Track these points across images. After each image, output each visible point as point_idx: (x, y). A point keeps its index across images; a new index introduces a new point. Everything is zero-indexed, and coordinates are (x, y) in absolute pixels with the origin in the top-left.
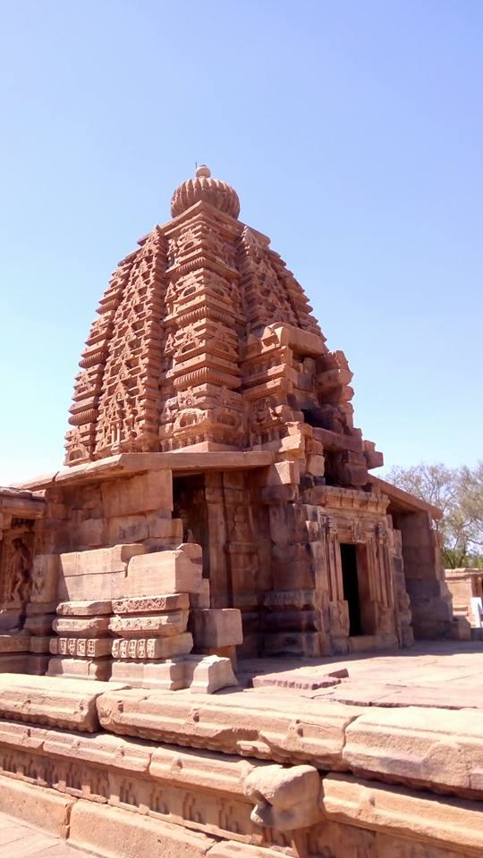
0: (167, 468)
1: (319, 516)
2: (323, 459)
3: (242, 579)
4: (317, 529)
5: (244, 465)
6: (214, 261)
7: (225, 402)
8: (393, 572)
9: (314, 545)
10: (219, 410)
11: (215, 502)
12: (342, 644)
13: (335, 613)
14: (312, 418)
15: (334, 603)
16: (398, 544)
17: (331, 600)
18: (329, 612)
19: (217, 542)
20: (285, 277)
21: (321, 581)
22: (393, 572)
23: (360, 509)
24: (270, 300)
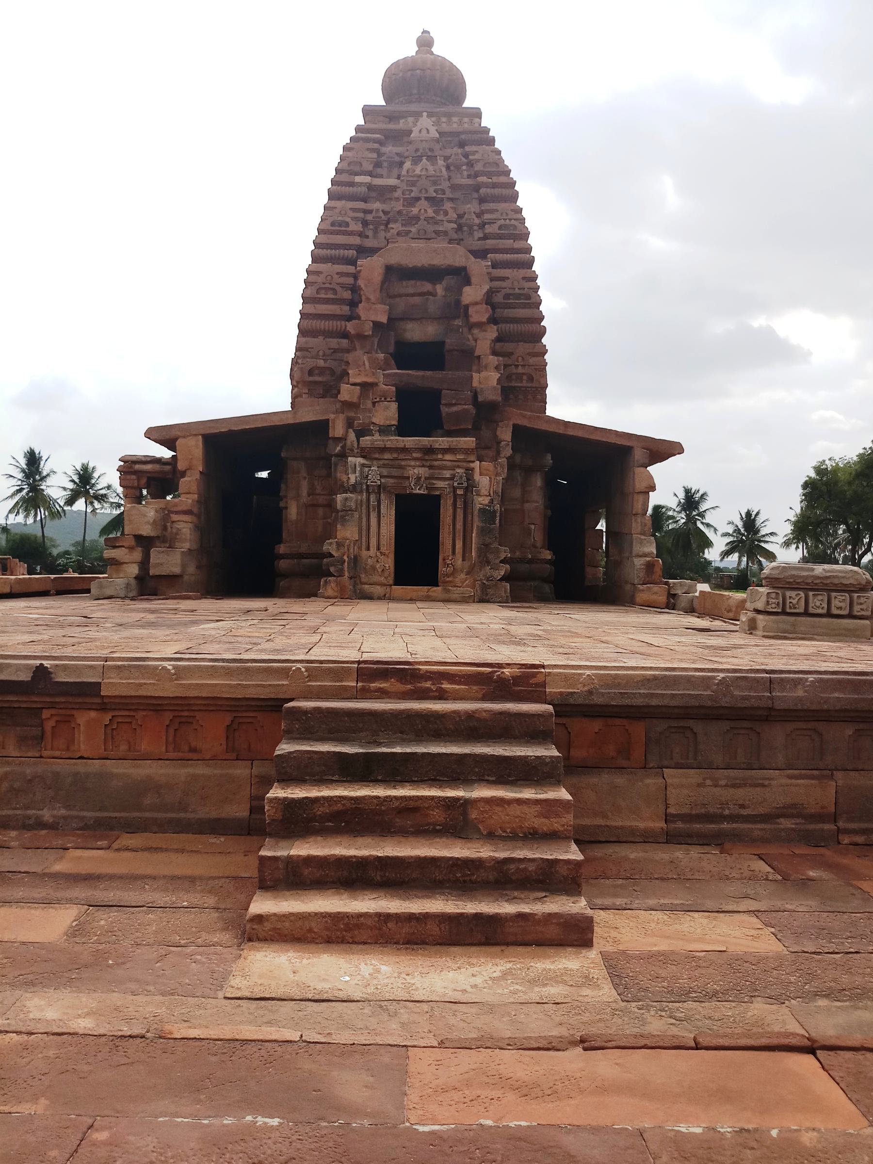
0: (196, 435)
1: (358, 469)
2: (394, 406)
3: (320, 529)
4: (353, 480)
5: (292, 422)
6: (352, 184)
7: (321, 353)
8: (477, 523)
9: (339, 498)
10: (311, 363)
11: (295, 459)
12: (378, 590)
13: (370, 561)
14: (408, 355)
15: (373, 551)
16: (495, 492)
17: (368, 549)
18: (356, 561)
19: (298, 497)
20: (478, 161)
21: (348, 532)
22: (477, 523)
23: (427, 457)
24: (415, 211)
